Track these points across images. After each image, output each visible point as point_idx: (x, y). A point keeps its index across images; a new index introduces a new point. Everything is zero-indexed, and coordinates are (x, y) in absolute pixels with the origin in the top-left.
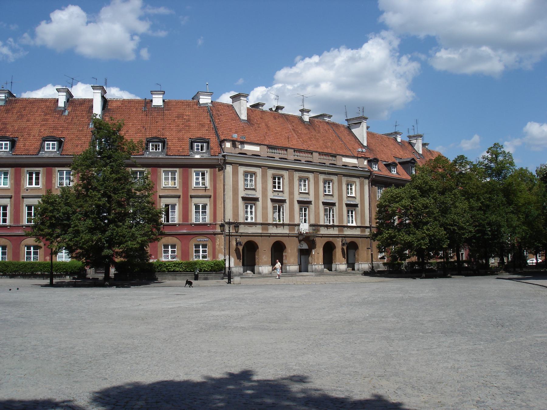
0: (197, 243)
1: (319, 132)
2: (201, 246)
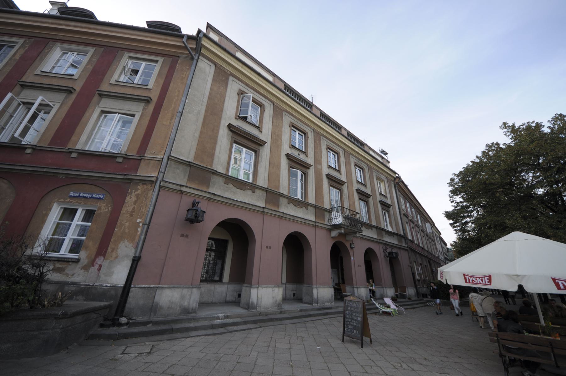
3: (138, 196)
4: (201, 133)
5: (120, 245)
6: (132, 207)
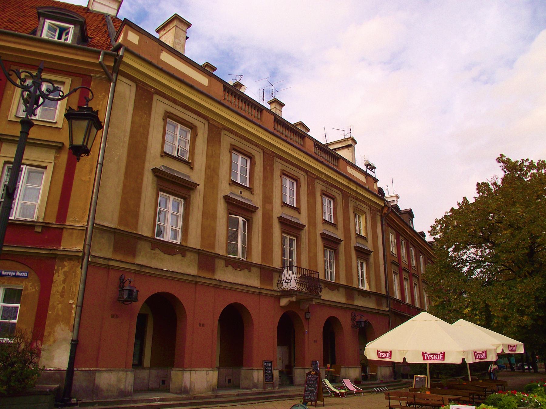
3: (65, 273)
4: (124, 186)
5: (56, 329)
6: (62, 287)
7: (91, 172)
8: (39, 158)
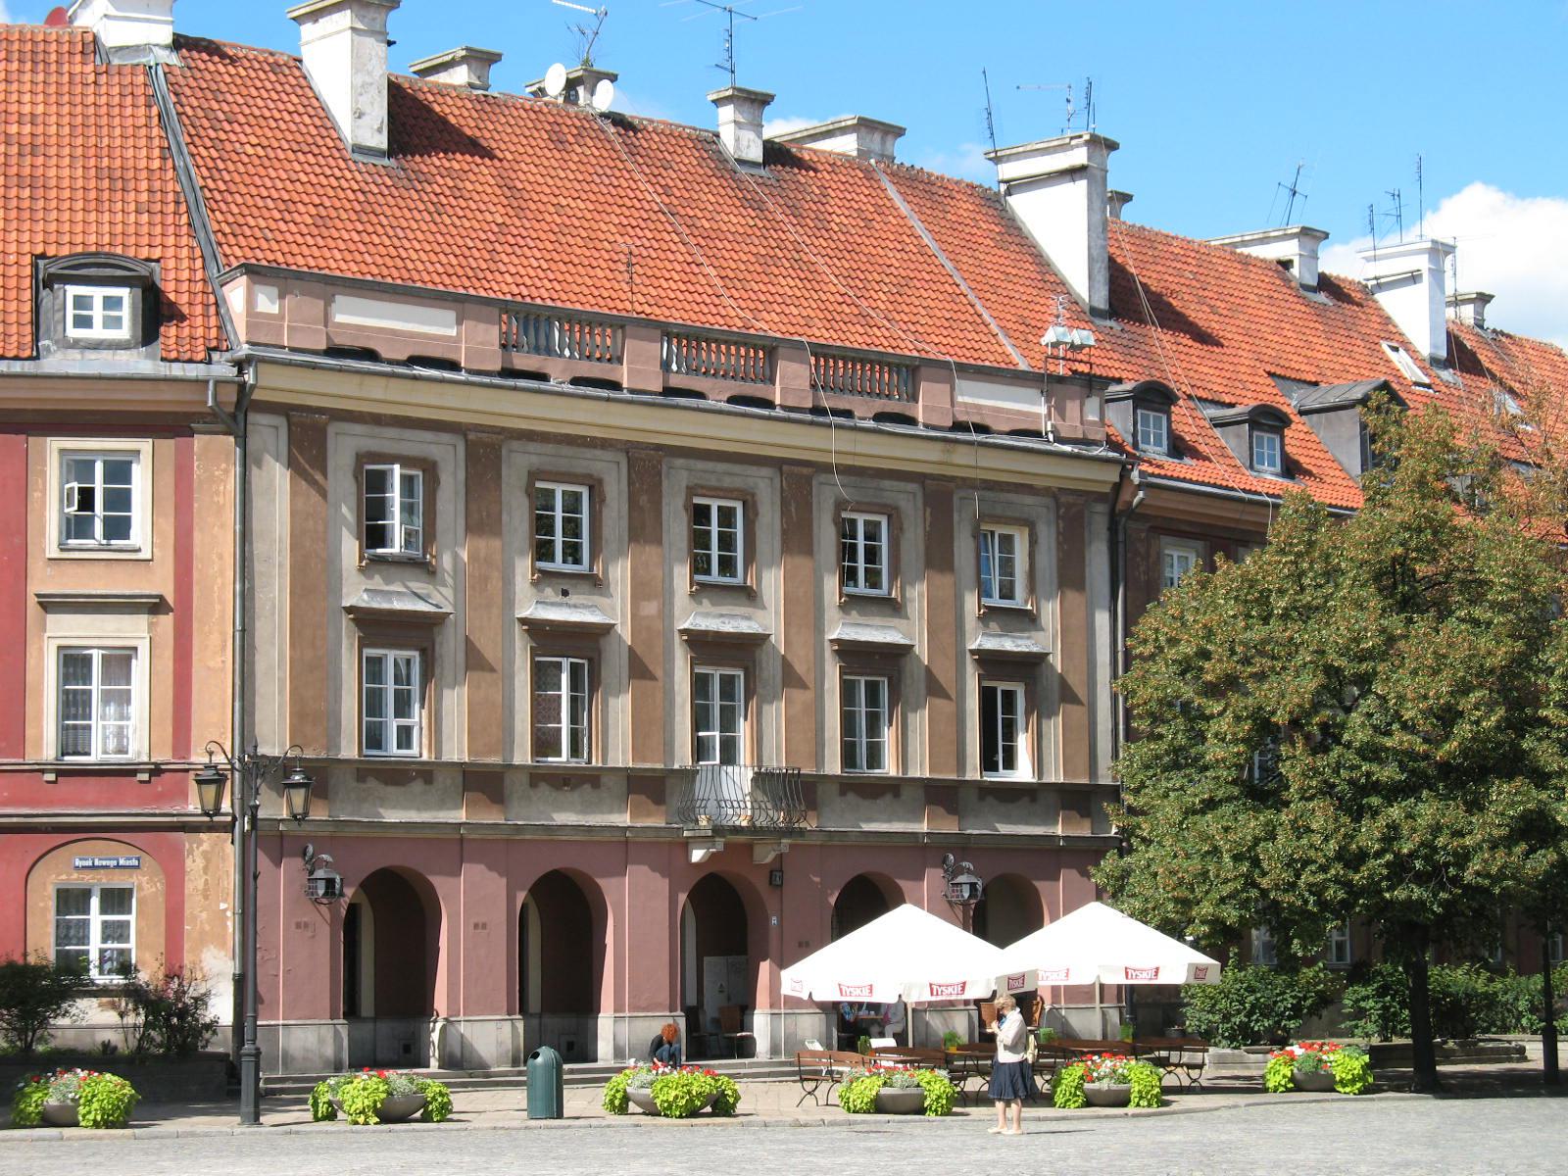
0: (75, 880)
1: (823, 225)
2: (95, 902)
3: (206, 855)
7: (224, 648)
8: (119, 631)
